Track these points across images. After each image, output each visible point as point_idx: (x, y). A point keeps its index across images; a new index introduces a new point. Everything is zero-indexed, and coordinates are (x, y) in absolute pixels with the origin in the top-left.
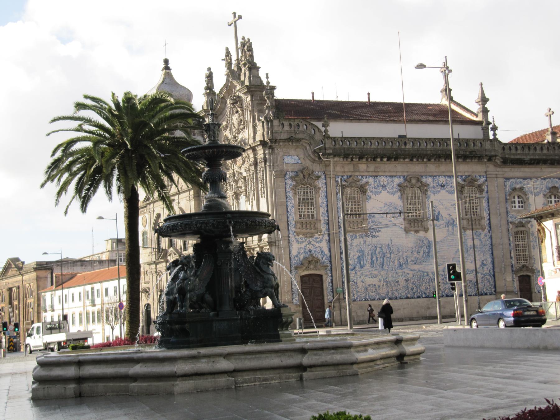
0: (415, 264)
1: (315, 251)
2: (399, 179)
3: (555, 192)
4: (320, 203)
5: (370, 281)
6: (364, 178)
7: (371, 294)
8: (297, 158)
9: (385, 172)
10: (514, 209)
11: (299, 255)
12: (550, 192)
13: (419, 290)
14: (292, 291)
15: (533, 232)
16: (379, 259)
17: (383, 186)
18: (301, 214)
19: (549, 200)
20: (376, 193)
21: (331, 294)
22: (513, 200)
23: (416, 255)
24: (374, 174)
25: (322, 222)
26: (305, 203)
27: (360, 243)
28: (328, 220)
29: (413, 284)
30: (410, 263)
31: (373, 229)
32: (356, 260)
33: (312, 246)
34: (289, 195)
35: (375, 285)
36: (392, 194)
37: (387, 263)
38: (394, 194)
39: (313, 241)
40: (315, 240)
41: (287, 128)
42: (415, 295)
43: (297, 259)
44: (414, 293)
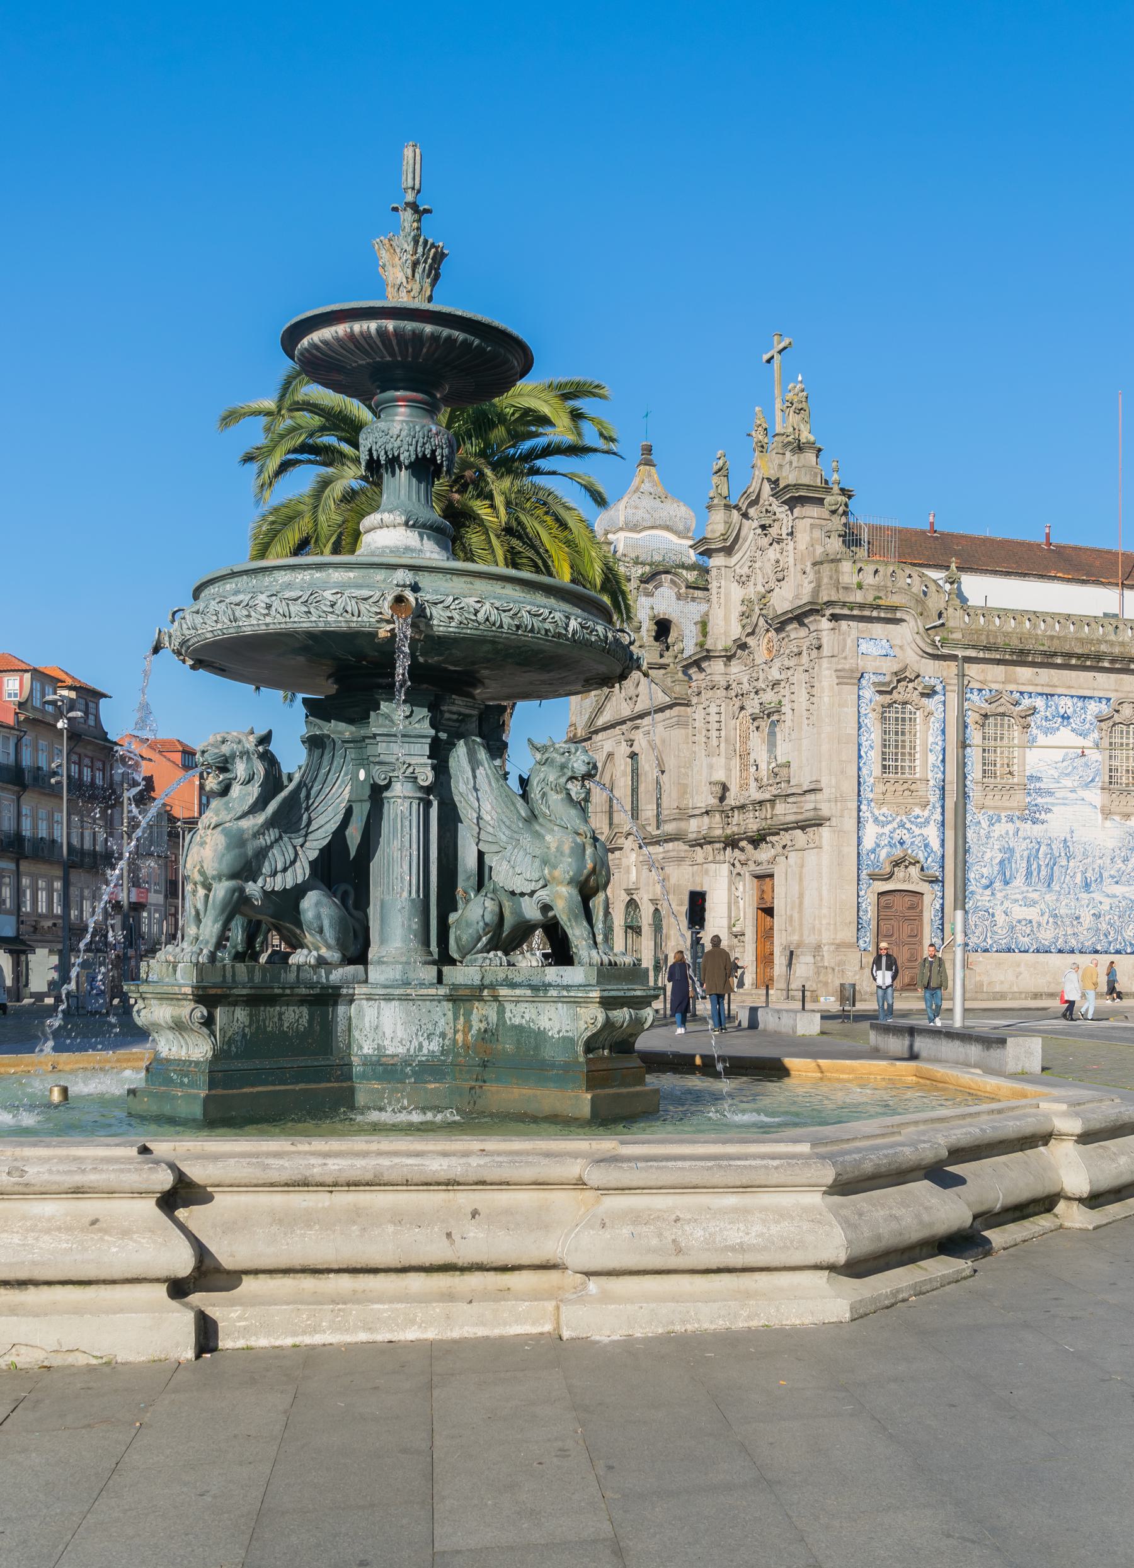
0: (1117, 883)
1: (912, 843)
2: (1098, 704)
4: (929, 743)
5: (1020, 912)
6: (1026, 697)
7: (1021, 938)
8: (887, 645)
9: (1069, 687)
11: (878, 850)
13: (1119, 938)
14: (858, 923)
16: (1043, 867)
17: (1063, 717)
20: (1047, 731)
21: (940, 934)
23: (1121, 865)
24: (1047, 690)
25: (932, 783)
26: (896, 741)
27: (1007, 833)
28: (944, 781)
29: (1109, 923)
31: (1036, 805)
32: (996, 868)
33: (905, 831)
34: (866, 721)
35: (1030, 922)
36: (1081, 735)
37: (1059, 879)
39: (910, 821)
40: (913, 819)
41: (869, 579)
42: (1111, 948)
43: (872, 856)
44: (1110, 943)
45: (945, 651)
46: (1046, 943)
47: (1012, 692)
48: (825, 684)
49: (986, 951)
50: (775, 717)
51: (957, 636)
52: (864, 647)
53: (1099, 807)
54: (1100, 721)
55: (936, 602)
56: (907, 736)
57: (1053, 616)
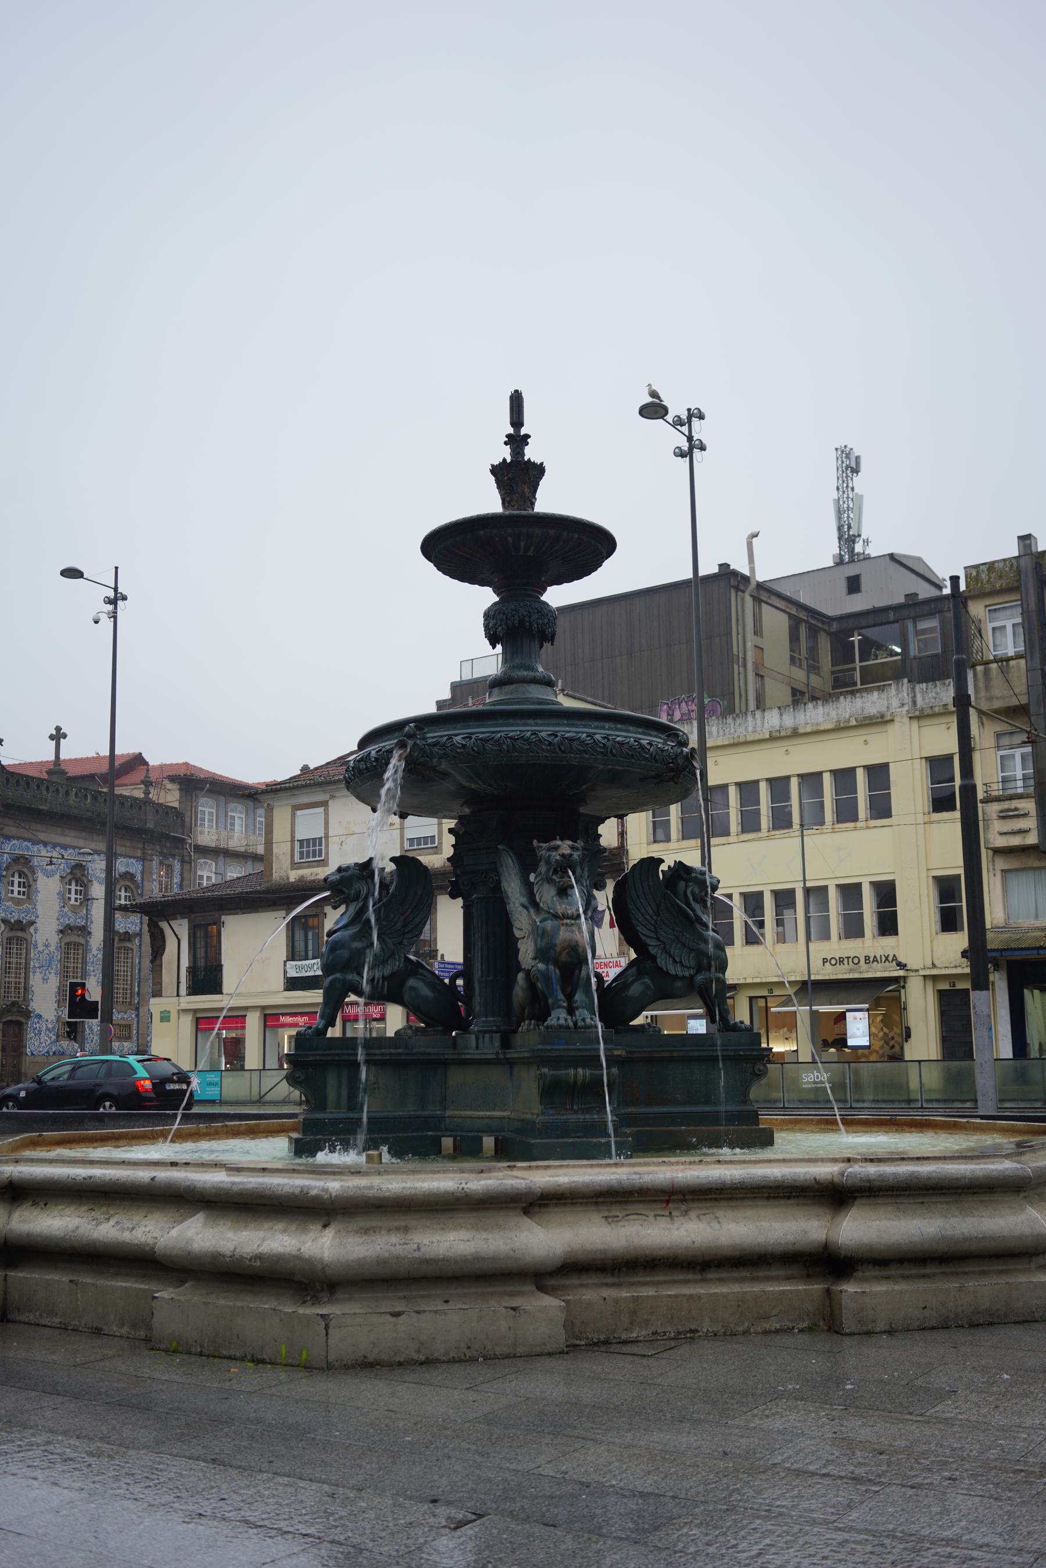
3: (79, 875)
10: (10, 895)
12: (71, 873)
15: (36, 941)
19: (68, 887)
22: (11, 879)
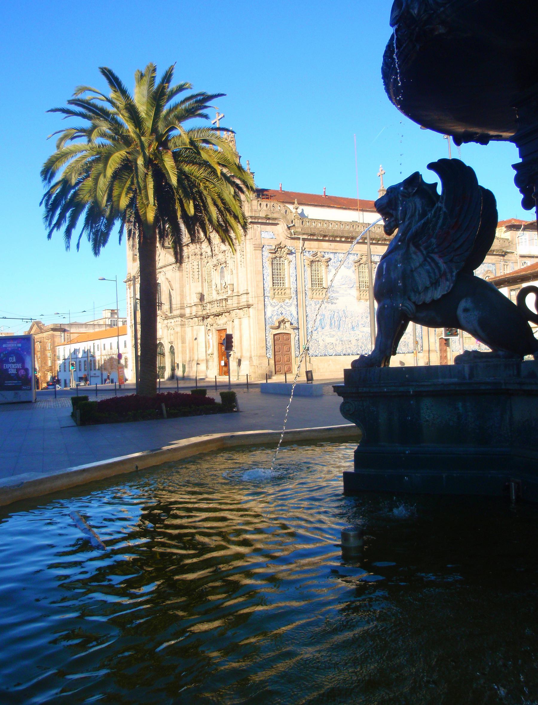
5: (329, 340)
16: (336, 322)
18: (274, 282)
23: (365, 319)
30: (360, 326)
33: (283, 309)
38: (349, 269)
39: (285, 305)
45: (296, 236)
46: (339, 352)
47: (321, 252)
48: (248, 250)
49: (316, 356)
50: (224, 265)
51: (299, 230)
52: (264, 235)
53: (356, 297)
54: (355, 263)
55: (291, 217)
56: (282, 271)
57: (335, 221)
